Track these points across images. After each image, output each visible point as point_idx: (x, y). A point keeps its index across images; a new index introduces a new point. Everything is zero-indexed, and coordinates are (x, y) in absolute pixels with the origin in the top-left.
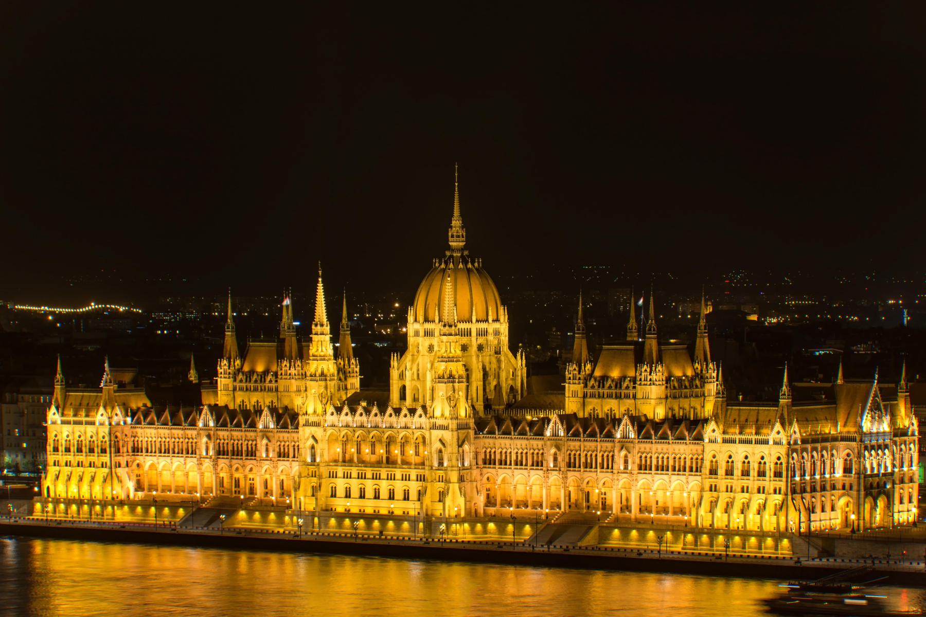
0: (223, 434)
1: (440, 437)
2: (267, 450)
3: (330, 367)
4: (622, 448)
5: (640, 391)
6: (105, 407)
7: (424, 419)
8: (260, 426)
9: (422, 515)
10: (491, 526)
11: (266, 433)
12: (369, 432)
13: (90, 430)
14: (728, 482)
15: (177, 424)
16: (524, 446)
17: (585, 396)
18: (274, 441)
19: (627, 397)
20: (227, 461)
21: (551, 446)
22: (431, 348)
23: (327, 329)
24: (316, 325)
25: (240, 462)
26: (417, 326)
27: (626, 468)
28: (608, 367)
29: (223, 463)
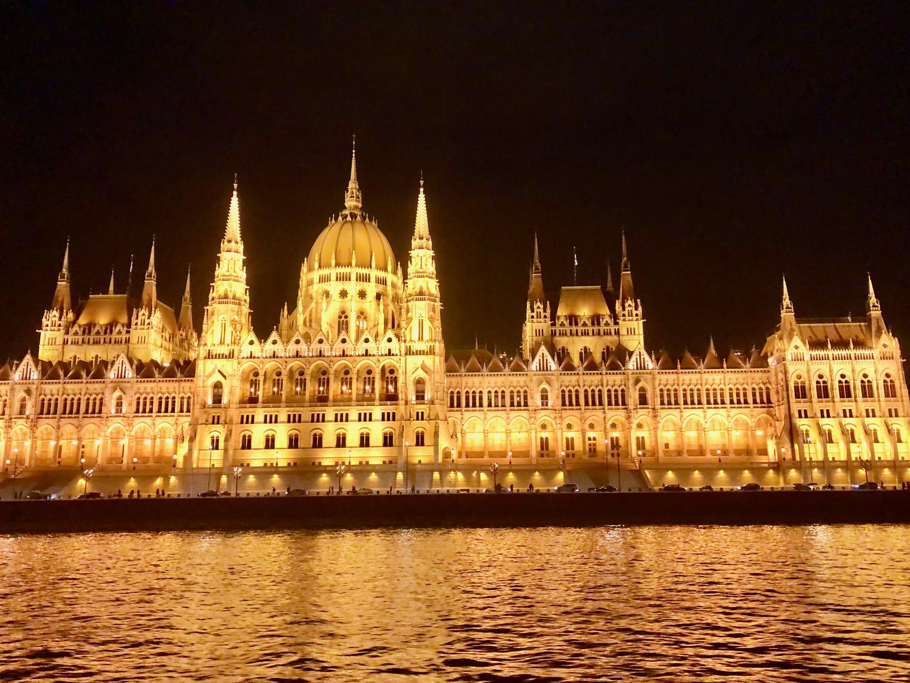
0: (52, 389)
2: (119, 405)
4: (637, 381)
5: (623, 326)
7: (395, 346)
8: (112, 374)
9: (401, 462)
12: (310, 363)
14: (825, 405)
16: (499, 384)
17: (553, 334)
18: (130, 392)
20: (53, 422)
21: (540, 383)
22: (344, 294)
23: (241, 247)
24: (229, 241)
25: (75, 421)
26: (325, 272)
27: (643, 400)
28: (573, 305)
29: (46, 425)
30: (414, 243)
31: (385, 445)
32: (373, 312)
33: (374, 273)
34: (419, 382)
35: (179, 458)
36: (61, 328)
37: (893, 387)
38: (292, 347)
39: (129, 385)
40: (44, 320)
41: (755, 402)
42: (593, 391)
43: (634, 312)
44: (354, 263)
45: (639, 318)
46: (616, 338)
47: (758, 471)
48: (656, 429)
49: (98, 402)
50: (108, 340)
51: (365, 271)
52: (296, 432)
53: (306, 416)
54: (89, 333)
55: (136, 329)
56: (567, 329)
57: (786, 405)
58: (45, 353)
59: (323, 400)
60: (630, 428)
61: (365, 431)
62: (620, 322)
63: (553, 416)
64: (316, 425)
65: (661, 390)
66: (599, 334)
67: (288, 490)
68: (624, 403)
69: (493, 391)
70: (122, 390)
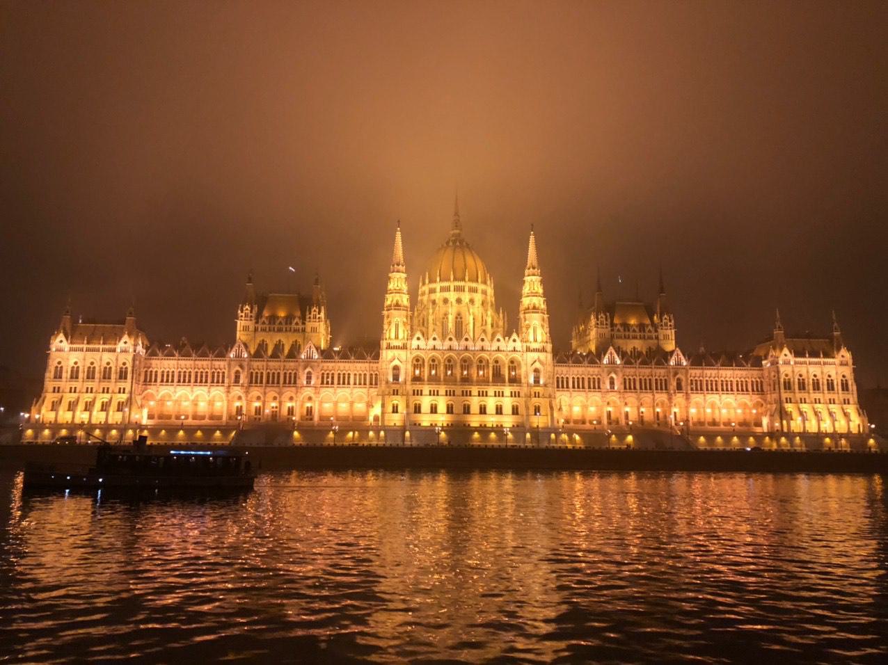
0: (257, 364)
1: (536, 357)
2: (309, 378)
3: (405, 300)
4: (676, 374)
5: (661, 332)
6: (129, 335)
7: (518, 345)
10: (577, 437)
11: (309, 361)
12: (460, 355)
13: (107, 357)
15: (204, 355)
16: (580, 373)
17: (612, 337)
19: (650, 338)
20: (262, 390)
21: (610, 373)
22: (459, 301)
24: (398, 265)
25: (277, 389)
26: (445, 284)
27: (679, 387)
29: (256, 392)
30: (527, 272)
31: (513, 414)
32: (480, 315)
33: (481, 287)
34: (536, 371)
35: (371, 419)
36: (253, 319)
37: (847, 384)
38: (447, 344)
39: (316, 364)
40: (239, 312)
41: (753, 390)
42: (645, 380)
43: (669, 324)
44: (467, 279)
45: (672, 327)
46: (656, 341)
47: (759, 438)
48: (687, 407)
49: (293, 376)
50: (288, 329)
51: (474, 285)
52: (452, 402)
53: (458, 392)
54: (274, 324)
55: (310, 321)
56: (622, 334)
57: (777, 392)
58: (241, 335)
59: (466, 380)
60: (670, 407)
61: (499, 404)
62: (659, 330)
63: (619, 396)
64: (465, 398)
65: (691, 380)
66: (644, 338)
67: (449, 443)
68: (666, 389)
69: (576, 377)
70: (311, 367)
